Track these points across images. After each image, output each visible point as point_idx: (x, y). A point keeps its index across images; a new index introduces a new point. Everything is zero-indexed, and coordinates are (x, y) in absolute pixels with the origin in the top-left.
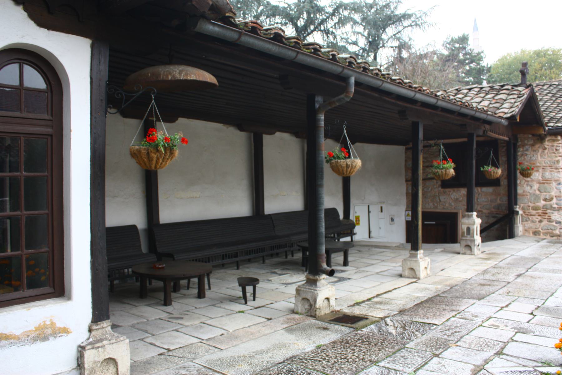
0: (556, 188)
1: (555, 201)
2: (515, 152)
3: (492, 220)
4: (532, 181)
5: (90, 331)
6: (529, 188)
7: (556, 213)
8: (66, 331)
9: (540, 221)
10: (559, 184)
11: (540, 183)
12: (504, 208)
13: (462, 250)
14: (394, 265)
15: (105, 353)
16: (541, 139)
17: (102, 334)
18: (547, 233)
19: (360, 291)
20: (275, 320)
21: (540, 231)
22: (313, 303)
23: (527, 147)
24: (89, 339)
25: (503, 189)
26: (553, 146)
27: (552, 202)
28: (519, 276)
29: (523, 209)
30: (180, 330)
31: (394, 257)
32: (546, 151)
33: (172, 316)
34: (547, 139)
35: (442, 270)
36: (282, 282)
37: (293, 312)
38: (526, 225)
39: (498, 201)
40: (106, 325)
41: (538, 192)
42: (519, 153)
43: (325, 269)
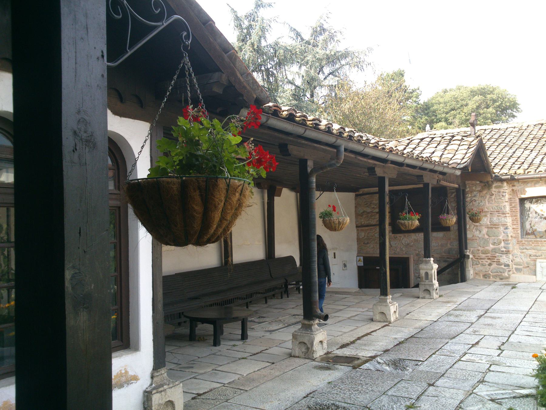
0: (504, 233)
1: (503, 244)
2: (464, 198)
3: (444, 265)
4: (481, 225)
5: (152, 377)
6: (478, 232)
7: (504, 256)
8: (135, 378)
9: (490, 265)
10: (507, 228)
11: (488, 228)
12: (454, 252)
13: (421, 294)
14: (361, 310)
15: (167, 396)
16: (487, 186)
17: (161, 379)
18: (496, 276)
19: (341, 335)
20: (278, 364)
21: (490, 274)
22: (309, 346)
23: (475, 193)
24: (151, 385)
25: (453, 234)
26: (499, 192)
27: (500, 246)
28: (480, 317)
29: (473, 253)
30: (197, 377)
31: (359, 303)
32: (493, 197)
33: (181, 366)
34: (494, 185)
35: (408, 314)
36: (264, 330)
37: (291, 356)
38: (477, 269)
39: (449, 246)
40: (163, 371)
41: (486, 237)
42: (468, 199)
43: (320, 314)
